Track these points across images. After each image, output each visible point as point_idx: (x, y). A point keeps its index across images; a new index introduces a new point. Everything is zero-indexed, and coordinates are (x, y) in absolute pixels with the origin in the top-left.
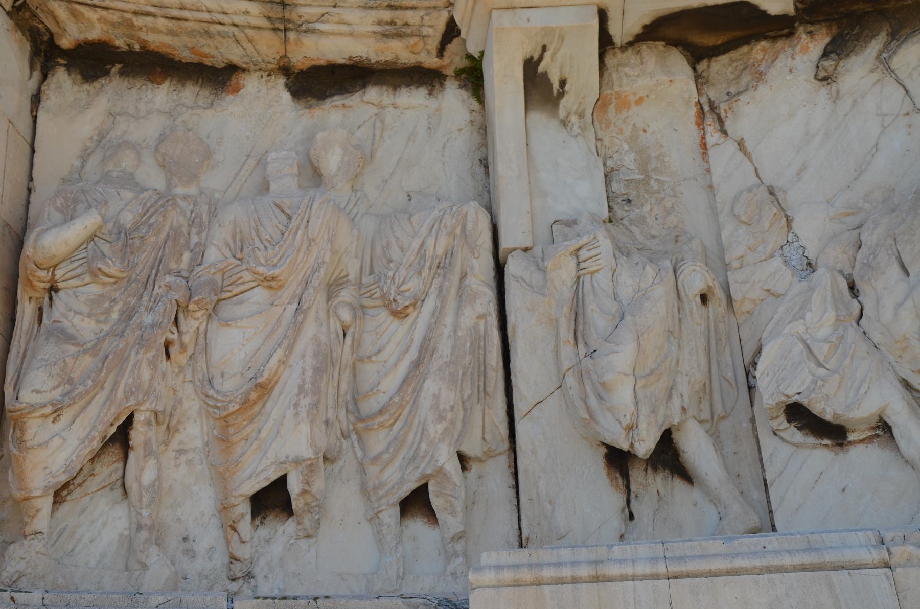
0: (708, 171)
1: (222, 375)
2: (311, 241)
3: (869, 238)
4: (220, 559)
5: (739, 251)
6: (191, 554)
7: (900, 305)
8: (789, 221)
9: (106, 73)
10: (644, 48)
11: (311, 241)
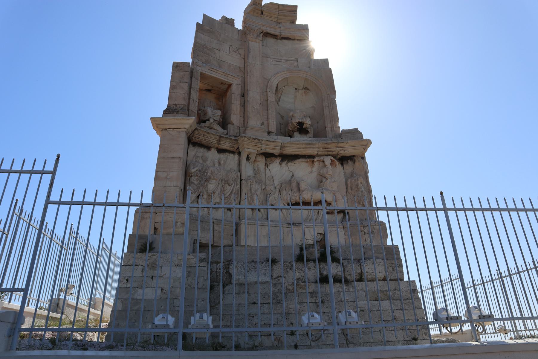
0: (265, 172)
2: (221, 175)
3: (282, 186)
4: (207, 212)
5: (268, 184)
6: (204, 211)
7: (285, 195)
10: (261, 156)
11: (221, 175)
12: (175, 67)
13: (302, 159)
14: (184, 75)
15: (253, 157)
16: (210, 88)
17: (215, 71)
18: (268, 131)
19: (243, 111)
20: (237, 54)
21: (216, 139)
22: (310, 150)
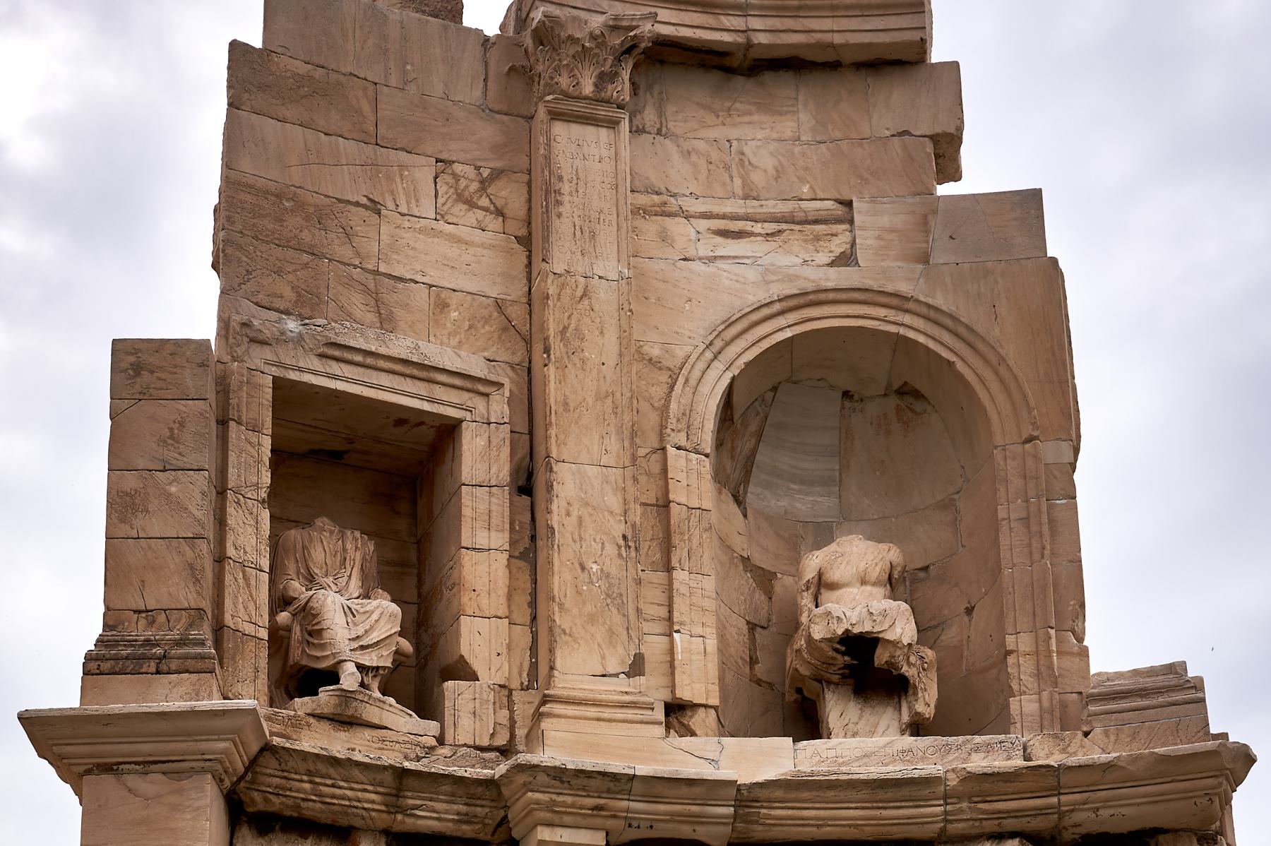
9: (272, 830)
12: (125, 371)
14: (182, 425)
16: (337, 445)
17: (359, 358)
18: (668, 697)
20: (480, 214)
21: (381, 784)
22: (901, 812)
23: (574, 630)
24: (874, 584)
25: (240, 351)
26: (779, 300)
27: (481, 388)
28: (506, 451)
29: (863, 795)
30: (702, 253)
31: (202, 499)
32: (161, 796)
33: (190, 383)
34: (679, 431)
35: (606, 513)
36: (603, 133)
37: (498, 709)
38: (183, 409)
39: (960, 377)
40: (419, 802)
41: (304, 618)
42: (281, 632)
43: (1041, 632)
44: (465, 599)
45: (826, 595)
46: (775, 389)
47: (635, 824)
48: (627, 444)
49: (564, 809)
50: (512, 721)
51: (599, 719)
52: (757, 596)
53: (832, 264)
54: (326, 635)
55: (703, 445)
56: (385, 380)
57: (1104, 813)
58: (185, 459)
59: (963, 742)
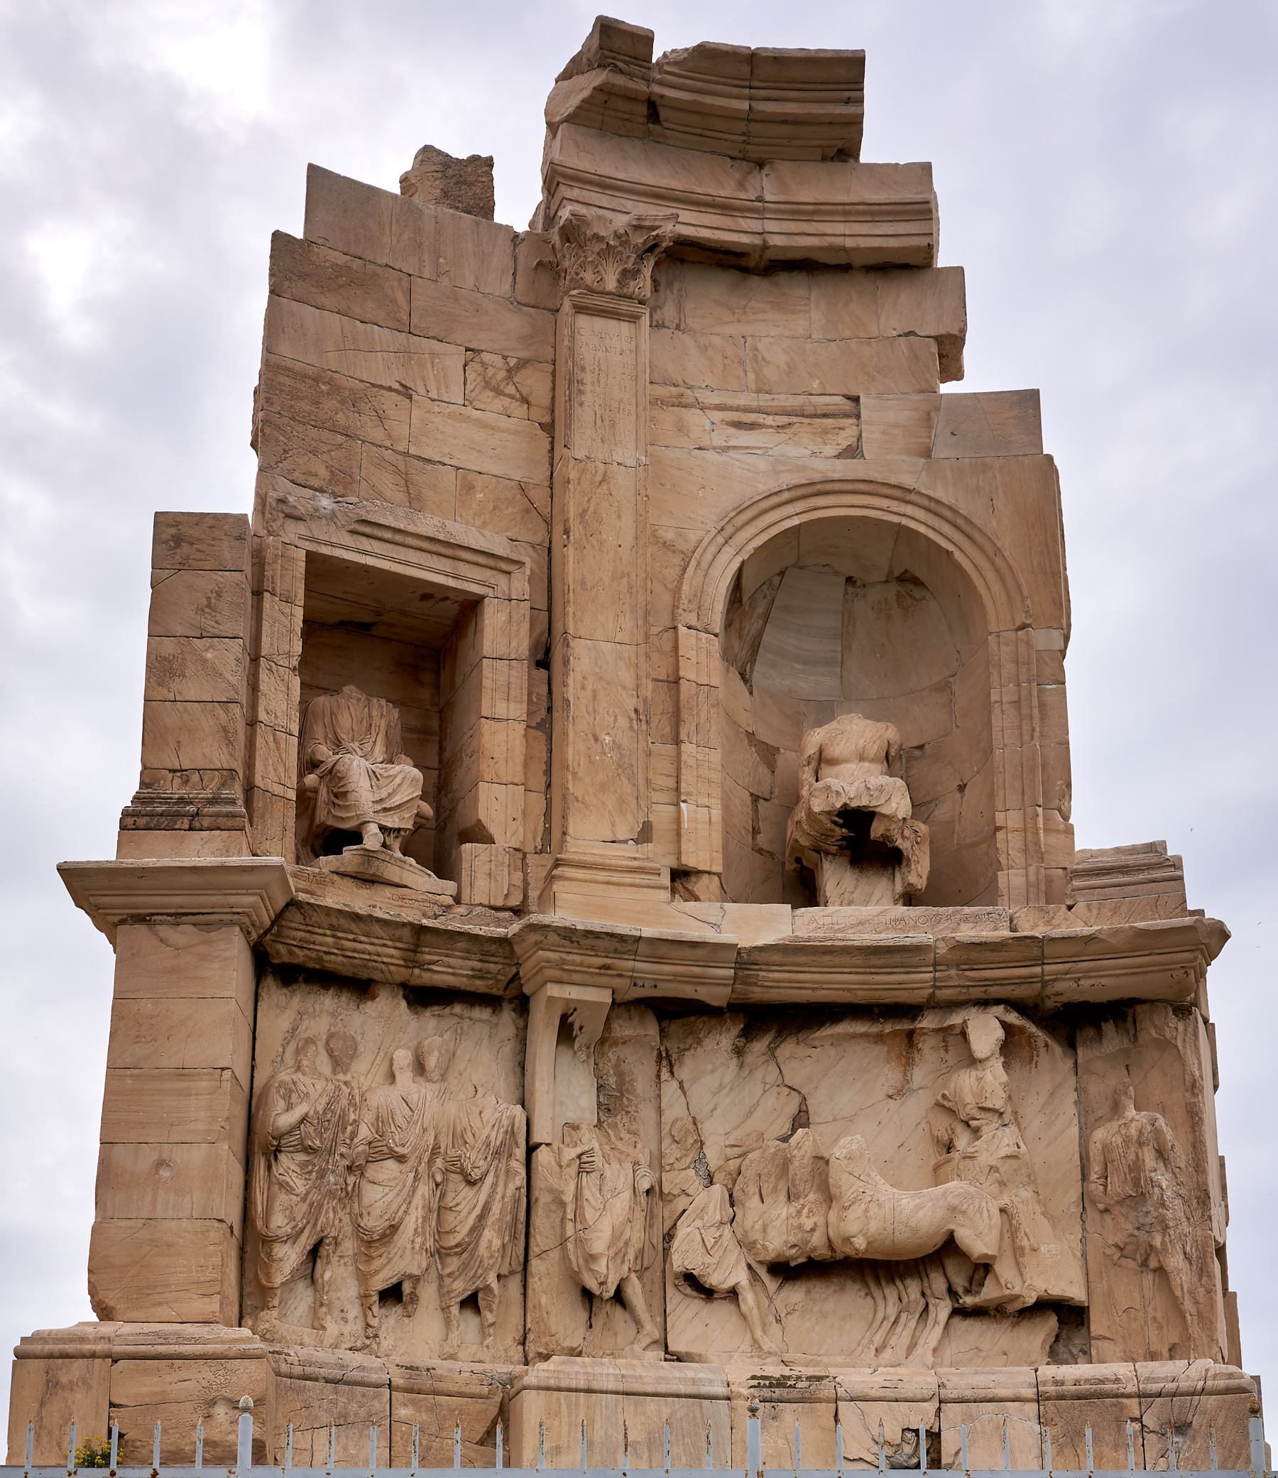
0: (659, 1096)
1: (369, 1214)
6: (345, 1320)
8: (702, 1143)
9: (294, 981)
12: (166, 542)
13: (853, 1024)
14: (219, 595)
15: (592, 1027)
16: (366, 617)
17: (388, 535)
18: (675, 865)
19: (544, 755)
20: (506, 401)
21: (400, 940)
23: (586, 798)
24: (872, 761)
25: (275, 526)
26: (788, 489)
27: (504, 566)
28: (526, 626)
29: (857, 960)
30: (716, 442)
31: (237, 666)
32: (191, 946)
33: (227, 556)
34: (690, 611)
35: (619, 688)
36: (625, 327)
37: (512, 871)
38: (220, 579)
39: (957, 566)
40: (435, 958)
41: (330, 780)
42: (309, 794)
43: (1029, 810)
44: (483, 766)
45: (826, 770)
46: (782, 573)
47: (640, 983)
48: (640, 622)
49: (573, 968)
50: (526, 883)
51: (608, 883)
52: (760, 770)
53: (838, 456)
54: (351, 797)
55: (713, 625)
56: (413, 556)
57: (1085, 983)
58: (221, 627)
59: (953, 912)
